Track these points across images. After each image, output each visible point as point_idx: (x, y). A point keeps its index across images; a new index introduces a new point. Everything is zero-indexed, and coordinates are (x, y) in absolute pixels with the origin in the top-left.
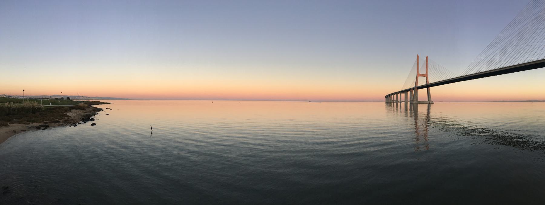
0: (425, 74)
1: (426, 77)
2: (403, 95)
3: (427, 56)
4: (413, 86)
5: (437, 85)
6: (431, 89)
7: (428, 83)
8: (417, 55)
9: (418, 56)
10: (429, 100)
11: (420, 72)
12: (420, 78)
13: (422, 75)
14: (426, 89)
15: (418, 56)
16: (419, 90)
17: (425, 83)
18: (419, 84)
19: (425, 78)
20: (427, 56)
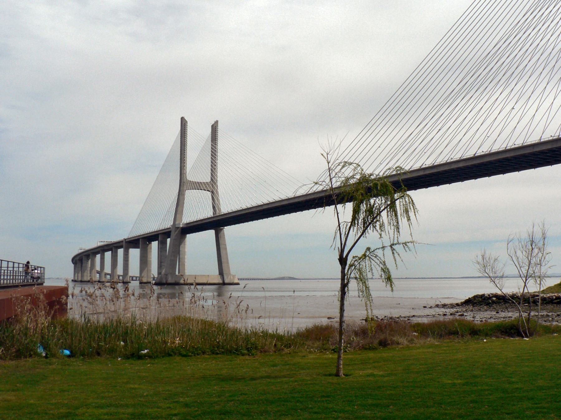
0: (208, 180)
1: (212, 192)
2: (135, 253)
3: (217, 122)
4: (168, 224)
5: (247, 221)
6: (229, 231)
7: (220, 209)
8: (182, 119)
9: (184, 123)
10: (221, 273)
11: (191, 176)
12: (190, 195)
13: (198, 186)
14: (211, 234)
15: (184, 123)
16: (188, 236)
17: (207, 213)
18: (188, 217)
19: (209, 194)
20: (217, 122)
